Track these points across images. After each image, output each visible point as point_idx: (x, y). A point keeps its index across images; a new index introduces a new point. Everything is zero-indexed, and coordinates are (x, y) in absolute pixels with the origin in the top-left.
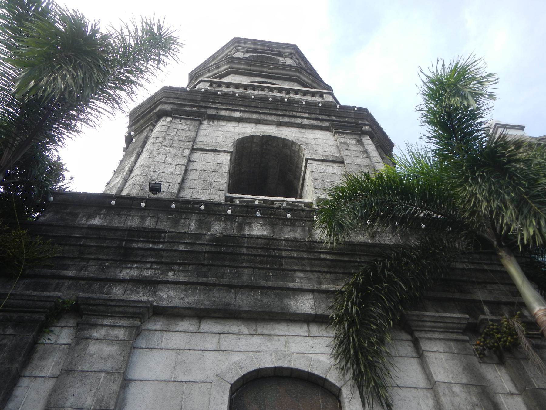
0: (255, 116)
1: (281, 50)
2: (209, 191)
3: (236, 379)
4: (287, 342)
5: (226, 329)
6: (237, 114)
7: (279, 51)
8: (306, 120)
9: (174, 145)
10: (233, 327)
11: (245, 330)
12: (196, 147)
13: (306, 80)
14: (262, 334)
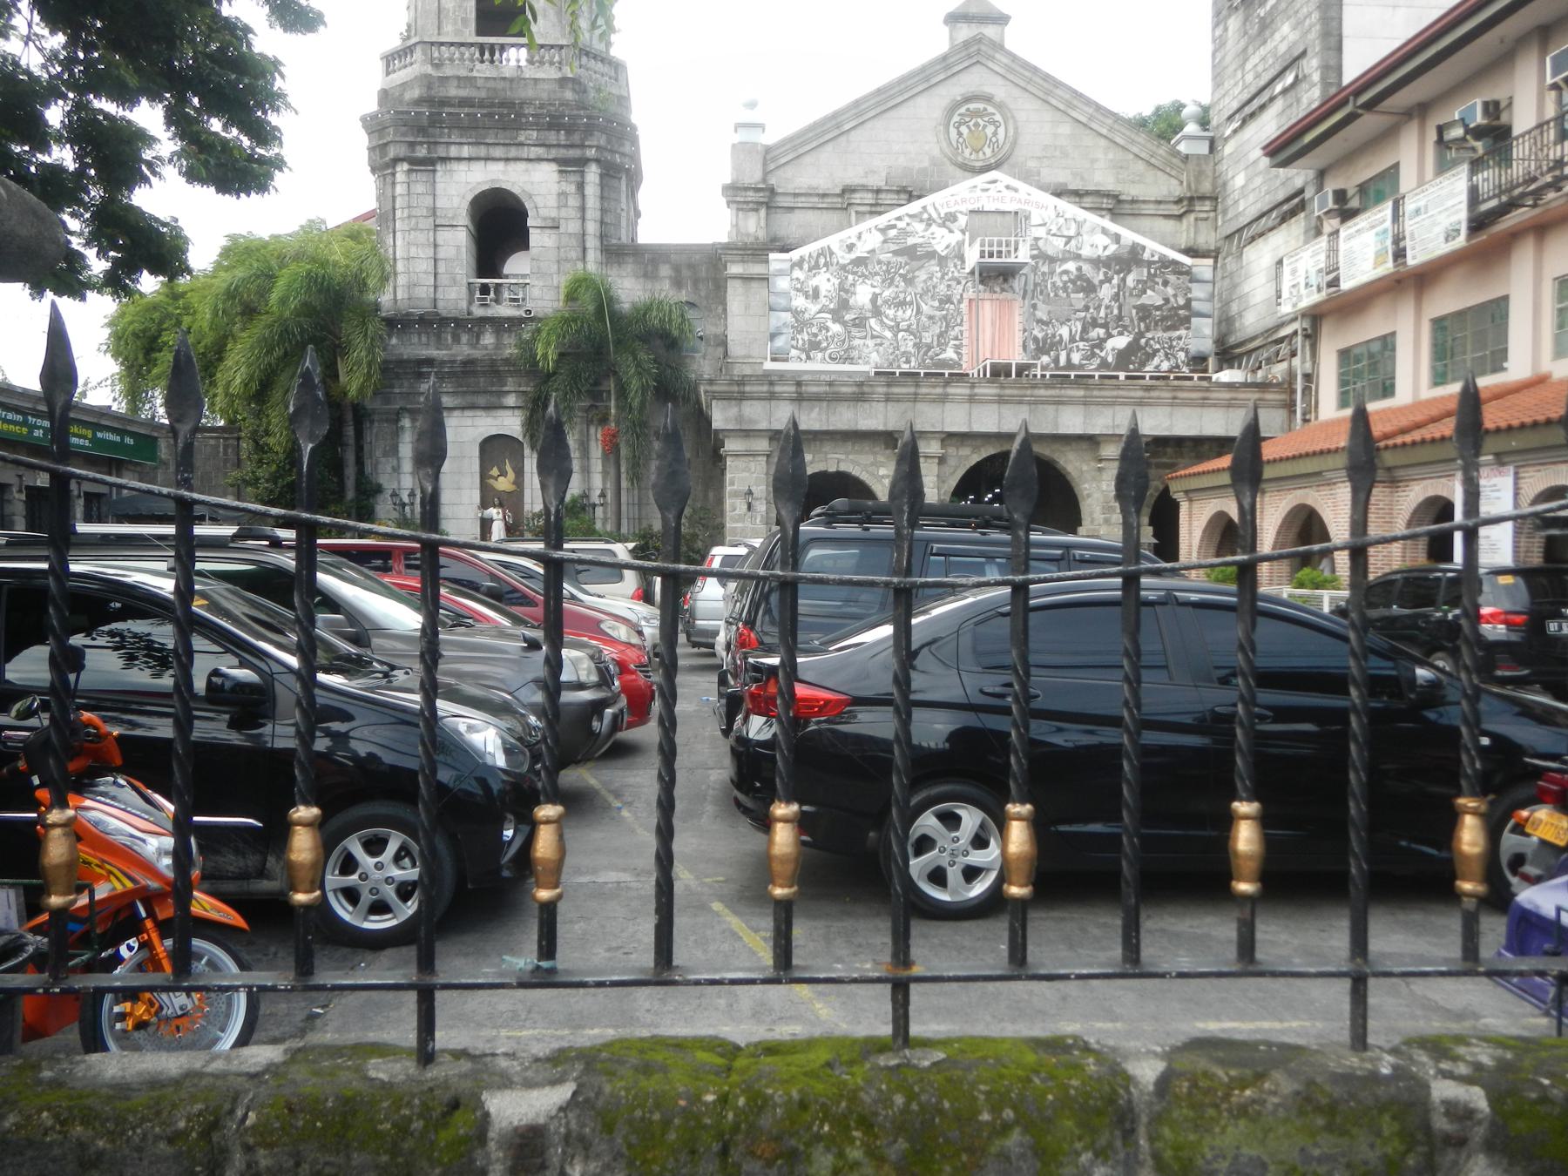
0: (482, 151)
6: (466, 151)
9: (420, 226)
10: (479, 413)
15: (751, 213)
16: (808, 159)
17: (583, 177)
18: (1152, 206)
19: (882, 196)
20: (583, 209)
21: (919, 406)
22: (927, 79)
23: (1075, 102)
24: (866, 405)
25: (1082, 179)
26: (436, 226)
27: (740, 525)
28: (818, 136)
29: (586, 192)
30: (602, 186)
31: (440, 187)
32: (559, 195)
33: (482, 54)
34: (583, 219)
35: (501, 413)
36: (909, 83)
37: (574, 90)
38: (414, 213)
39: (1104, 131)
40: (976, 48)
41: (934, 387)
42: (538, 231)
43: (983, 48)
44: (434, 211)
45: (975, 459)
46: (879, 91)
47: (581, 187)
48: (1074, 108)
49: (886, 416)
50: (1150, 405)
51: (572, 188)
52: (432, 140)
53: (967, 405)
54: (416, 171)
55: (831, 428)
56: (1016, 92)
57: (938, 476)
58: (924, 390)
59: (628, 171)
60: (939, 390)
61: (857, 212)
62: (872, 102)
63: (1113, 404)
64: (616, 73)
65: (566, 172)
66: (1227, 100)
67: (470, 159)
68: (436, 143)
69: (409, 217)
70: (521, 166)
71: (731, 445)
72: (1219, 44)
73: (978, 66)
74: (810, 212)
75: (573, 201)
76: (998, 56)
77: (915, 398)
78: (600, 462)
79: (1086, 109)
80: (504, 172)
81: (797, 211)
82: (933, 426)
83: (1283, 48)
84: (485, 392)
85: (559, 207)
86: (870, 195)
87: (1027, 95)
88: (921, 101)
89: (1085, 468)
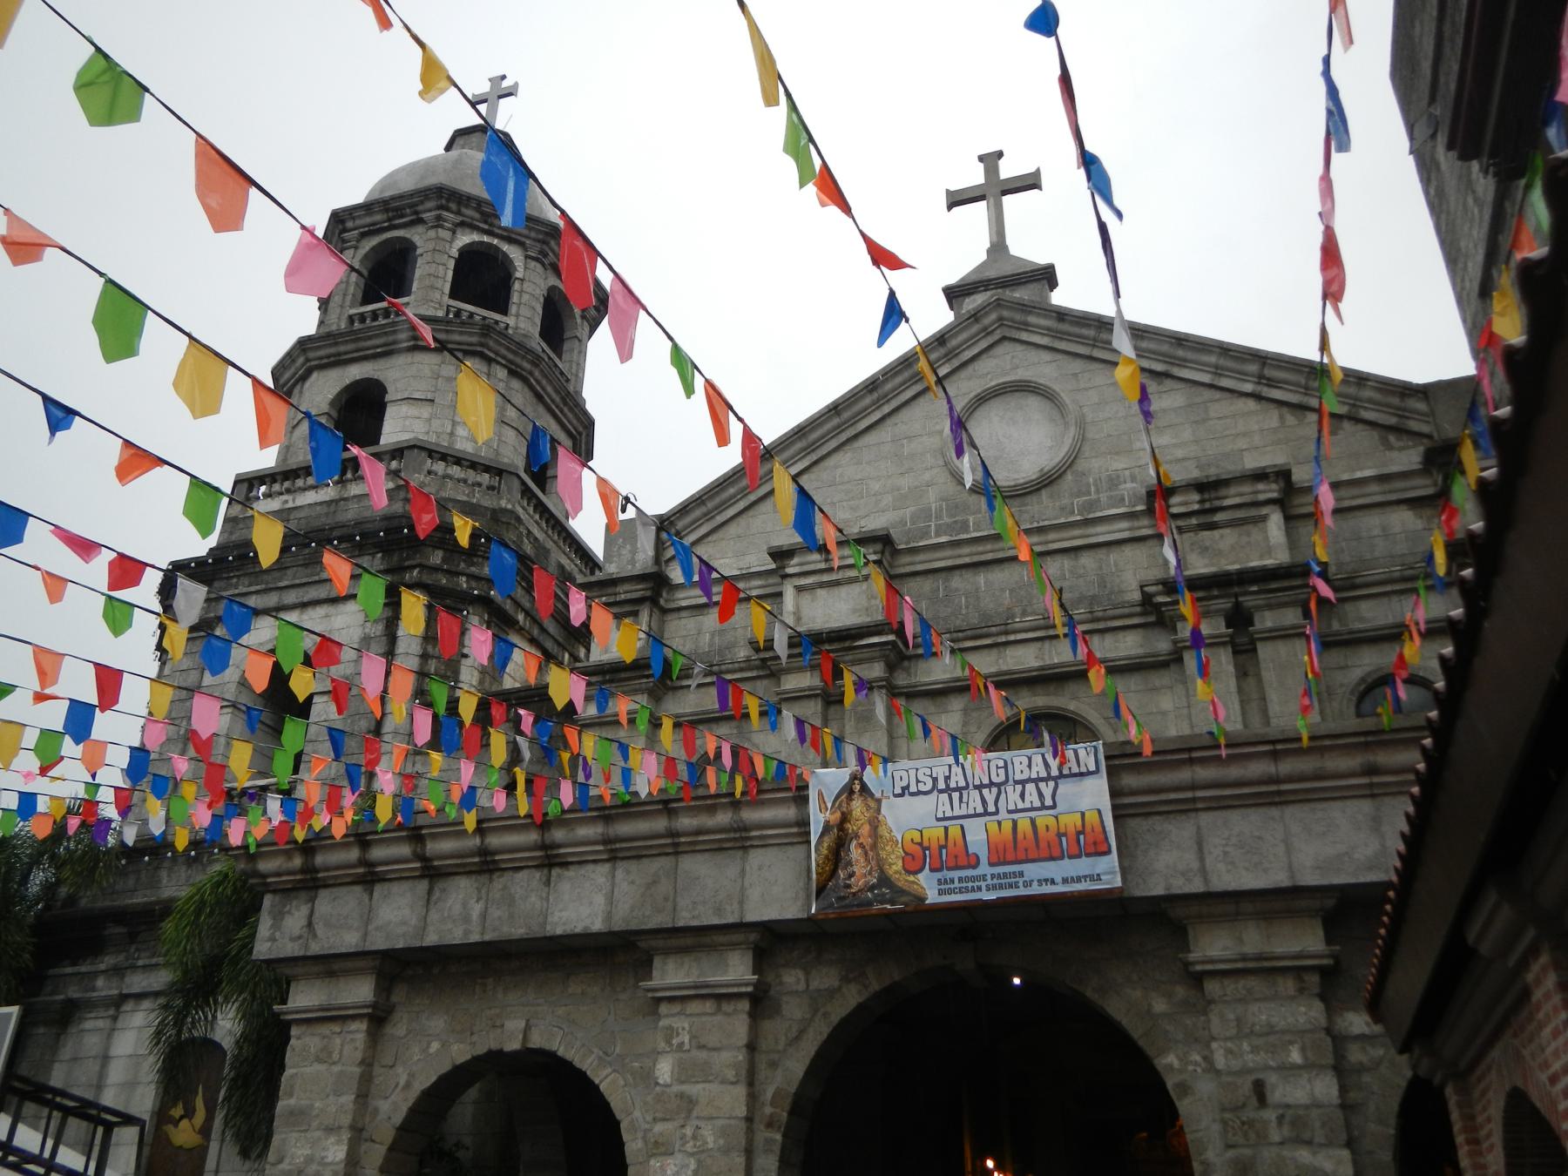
7: (416, 213)
16: (732, 529)
18: (1374, 488)
21: (689, 864)
23: (1180, 353)
24: (571, 873)
25: (1218, 467)
29: (400, 633)
36: (889, 386)
39: (1248, 387)
40: (993, 316)
41: (712, 810)
43: (1006, 313)
45: (852, 997)
46: (835, 409)
48: (1183, 363)
50: (1305, 798)
55: (487, 938)
56: (1077, 365)
57: (751, 1047)
58: (686, 822)
59: (485, 602)
60: (723, 818)
61: (800, 589)
63: (1187, 808)
66: (1470, 265)
70: (321, 611)
71: (304, 997)
72: (1437, 204)
76: (1032, 319)
77: (675, 844)
82: (719, 911)
89: (1160, 1006)
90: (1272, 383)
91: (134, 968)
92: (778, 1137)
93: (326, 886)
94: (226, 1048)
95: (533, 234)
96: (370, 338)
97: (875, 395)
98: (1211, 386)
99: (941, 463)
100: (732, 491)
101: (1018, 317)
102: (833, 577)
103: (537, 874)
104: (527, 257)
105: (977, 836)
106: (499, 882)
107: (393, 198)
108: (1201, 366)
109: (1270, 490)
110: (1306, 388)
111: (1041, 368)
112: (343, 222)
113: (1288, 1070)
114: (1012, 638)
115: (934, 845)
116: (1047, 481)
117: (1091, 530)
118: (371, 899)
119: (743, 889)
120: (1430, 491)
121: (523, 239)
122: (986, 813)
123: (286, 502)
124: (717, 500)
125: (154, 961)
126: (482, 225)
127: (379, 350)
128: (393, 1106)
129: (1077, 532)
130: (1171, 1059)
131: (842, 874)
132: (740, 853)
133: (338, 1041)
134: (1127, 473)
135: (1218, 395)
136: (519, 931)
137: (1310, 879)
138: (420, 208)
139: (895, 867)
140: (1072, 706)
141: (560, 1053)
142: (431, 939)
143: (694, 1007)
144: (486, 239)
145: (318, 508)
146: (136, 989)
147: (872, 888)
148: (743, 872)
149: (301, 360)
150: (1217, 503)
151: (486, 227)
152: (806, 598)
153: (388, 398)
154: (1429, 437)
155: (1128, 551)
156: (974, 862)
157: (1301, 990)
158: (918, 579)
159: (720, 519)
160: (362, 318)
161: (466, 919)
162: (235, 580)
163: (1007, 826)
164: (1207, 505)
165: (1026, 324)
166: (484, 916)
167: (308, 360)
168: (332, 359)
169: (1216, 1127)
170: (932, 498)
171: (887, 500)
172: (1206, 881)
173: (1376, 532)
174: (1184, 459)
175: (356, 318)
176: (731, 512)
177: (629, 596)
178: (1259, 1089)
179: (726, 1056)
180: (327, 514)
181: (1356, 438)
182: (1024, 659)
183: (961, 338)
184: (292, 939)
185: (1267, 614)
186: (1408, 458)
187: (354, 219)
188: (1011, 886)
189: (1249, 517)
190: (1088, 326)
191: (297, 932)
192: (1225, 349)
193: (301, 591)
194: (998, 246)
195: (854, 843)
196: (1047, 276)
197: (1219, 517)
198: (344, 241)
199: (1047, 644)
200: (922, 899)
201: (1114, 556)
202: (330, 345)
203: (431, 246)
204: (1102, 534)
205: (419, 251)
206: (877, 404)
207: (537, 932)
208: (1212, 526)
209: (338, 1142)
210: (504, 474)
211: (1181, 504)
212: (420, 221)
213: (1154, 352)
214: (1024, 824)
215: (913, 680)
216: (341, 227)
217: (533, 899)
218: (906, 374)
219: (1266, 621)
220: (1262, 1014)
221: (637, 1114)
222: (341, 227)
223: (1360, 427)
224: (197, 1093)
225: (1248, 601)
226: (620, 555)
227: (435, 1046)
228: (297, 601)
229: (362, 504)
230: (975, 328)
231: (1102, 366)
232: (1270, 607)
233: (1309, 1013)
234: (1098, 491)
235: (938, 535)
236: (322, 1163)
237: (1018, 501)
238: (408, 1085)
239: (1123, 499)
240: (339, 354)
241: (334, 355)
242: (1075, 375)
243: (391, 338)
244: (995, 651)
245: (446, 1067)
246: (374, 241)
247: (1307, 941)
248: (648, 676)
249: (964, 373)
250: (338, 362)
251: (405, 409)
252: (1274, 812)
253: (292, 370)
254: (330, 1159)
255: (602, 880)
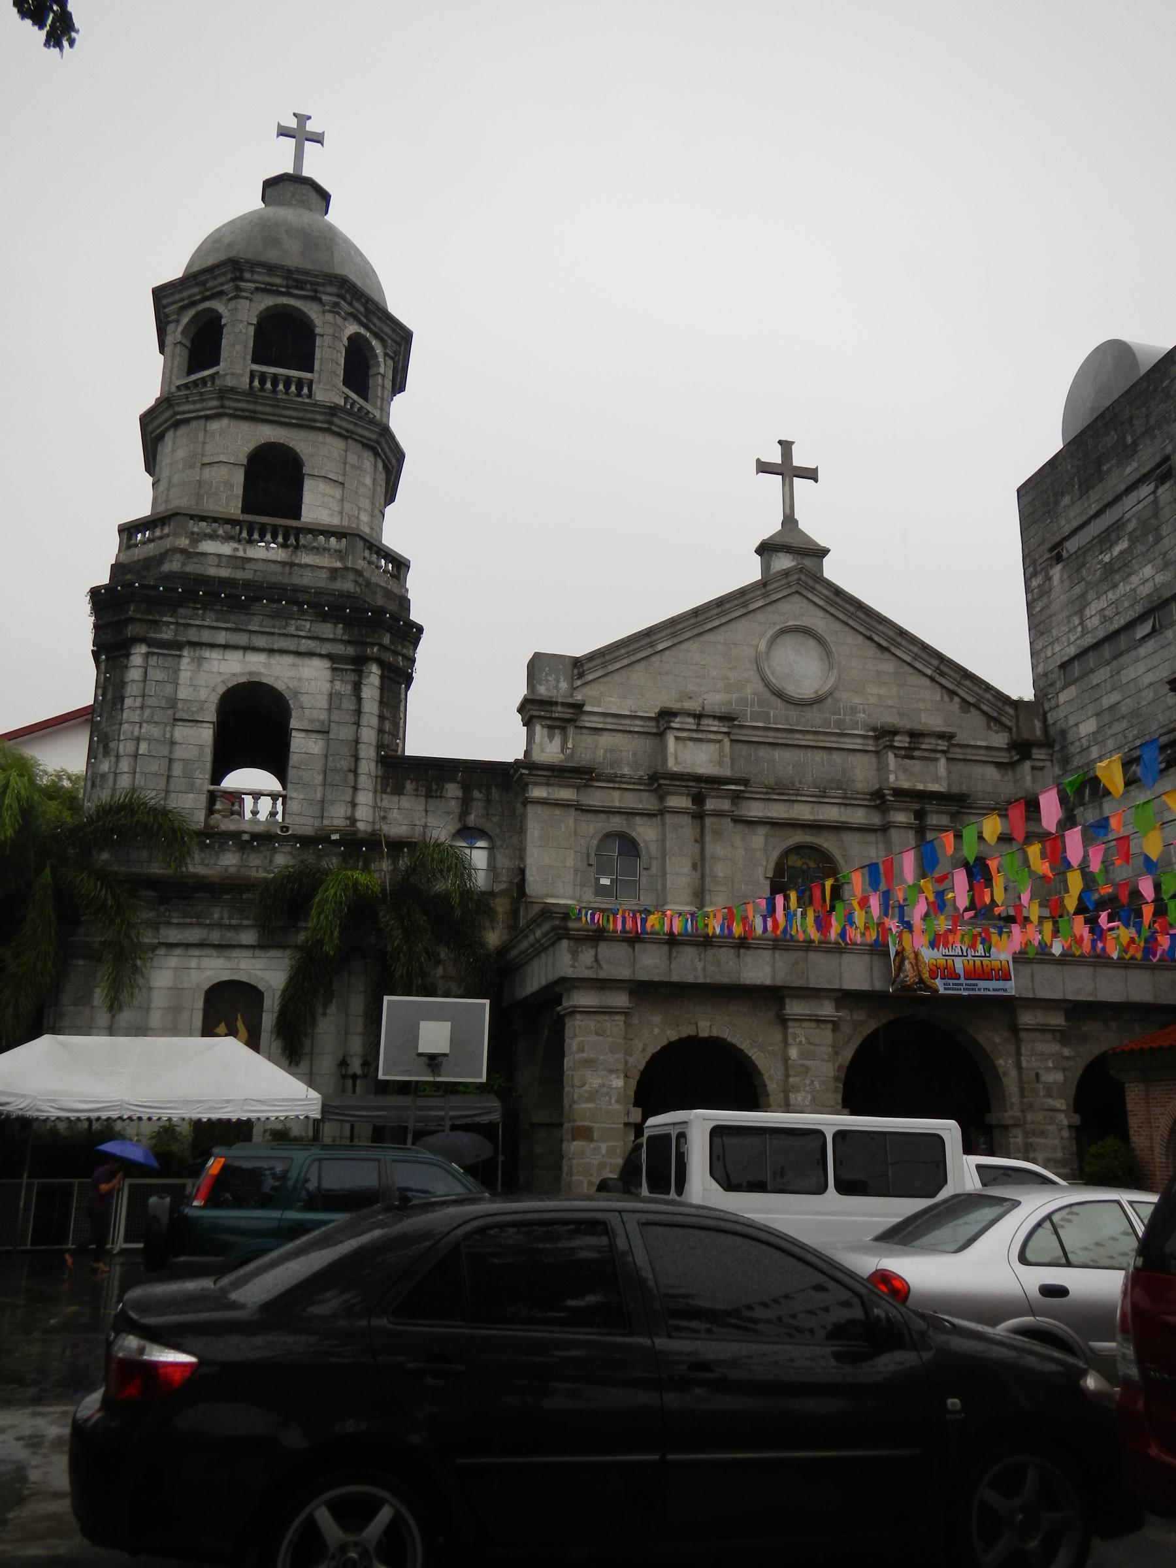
0: (242, 639)
1: (321, 289)
2: (191, 796)
3: (208, 987)
4: (239, 962)
5: (203, 953)
6: (221, 637)
7: (316, 291)
8: (304, 641)
9: (156, 719)
11: (215, 954)
12: (177, 717)
13: (345, 425)
14: (225, 957)
15: (557, 731)
16: (617, 678)
17: (360, 677)
18: (983, 752)
19: (704, 721)
20: (358, 712)
21: (812, 956)
22: (745, 604)
24: (751, 952)
26: (176, 720)
27: (590, 1105)
28: (629, 654)
29: (364, 695)
30: (382, 689)
31: (185, 675)
32: (331, 695)
33: (250, 534)
34: (358, 724)
35: (236, 953)
36: (728, 606)
37: (355, 581)
38: (149, 702)
39: (929, 672)
42: (303, 735)
43: (803, 577)
44: (173, 702)
45: (872, 1026)
46: (696, 612)
47: (357, 688)
49: (773, 968)
51: (348, 689)
52: (181, 621)
53: (867, 958)
54: (159, 654)
55: (708, 981)
56: (837, 626)
61: (677, 738)
62: (689, 622)
64: (399, 570)
65: (342, 670)
66: (1057, 648)
67: (226, 647)
68: (187, 625)
69: (142, 707)
70: (287, 660)
73: (797, 595)
74: (620, 735)
75: (349, 704)
76: (818, 587)
78: (360, 1021)
79: (912, 648)
80: (268, 665)
81: (606, 733)
83: (1145, 590)
84: (220, 925)
85: (329, 710)
86: (691, 720)
87: (847, 629)
88: (741, 627)
90: (942, 674)
91: (168, 924)
92: (841, 1086)
93: (605, 939)
94: (262, 990)
95: (394, 336)
96: (289, 408)
97: (720, 610)
98: (909, 664)
99: (755, 668)
100: (623, 651)
101: (811, 582)
102: (700, 736)
103: (732, 951)
104: (386, 354)
105: (959, 965)
106: (710, 952)
107: (298, 271)
108: (907, 651)
109: (943, 745)
110: (959, 683)
111: (817, 621)
112: (241, 271)
113: (1048, 1069)
114: (799, 798)
115: (942, 967)
116: (818, 701)
117: (842, 740)
118: (634, 951)
119: (841, 972)
120: (1006, 761)
121: (386, 338)
122: (963, 956)
123: (236, 550)
124: (613, 656)
125: (188, 920)
126: (363, 318)
127: (294, 421)
128: (640, 1061)
129: (834, 739)
130: (1001, 1062)
131: (902, 975)
132: (837, 954)
133: (608, 1025)
134: (861, 707)
135: (912, 671)
136: (725, 980)
137: (1070, 997)
138: (321, 289)
139: (926, 975)
140: (826, 845)
141: (729, 1039)
142: (675, 978)
143: (805, 1024)
144: (362, 331)
145: (273, 566)
146: (171, 940)
147: (916, 984)
148: (840, 964)
149: (215, 403)
150: (917, 745)
151: (365, 321)
152: (680, 744)
153: (305, 470)
154: (1010, 729)
155: (859, 757)
156: (957, 977)
157: (1054, 1038)
158: (739, 744)
159: (611, 668)
160: (263, 378)
161: (695, 970)
162: (201, 612)
163: (971, 963)
164: (912, 746)
165: (814, 588)
166: (704, 969)
167: (223, 406)
168: (247, 414)
169: (1016, 1089)
170: (749, 690)
171: (720, 685)
172: (1034, 994)
173: (980, 777)
174: (891, 707)
175: (257, 374)
176: (618, 665)
177: (561, 715)
178: (1037, 1076)
179: (823, 1049)
180: (283, 574)
181: (976, 718)
182: (804, 812)
183: (775, 585)
184: (586, 968)
185: (934, 816)
186: (1000, 740)
187: (253, 272)
188: (973, 990)
189: (930, 758)
190: (851, 604)
191: (589, 964)
192: (925, 647)
193: (270, 639)
194: (789, 520)
195: (906, 962)
196: (824, 552)
197: (916, 753)
198: (238, 288)
199: (816, 806)
200: (937, 991)
201: (851, 758)
202: (249, 402)
203: (329, 330)
204: (848, 743)
205: (318, 331)
206: (719, 615)
207: (735, 981)
208: (911, 758)
209: (618, 1078)
210: (403, 567)
211: (899, 741)
212: (319, 300)
213: (884, 634)
214: (978, 963)
215: (741, 813)
216: (238, 274)
217: (731, 963)
218: (740, 601)
219: (933, 820)
220: (1041, 1047)
221: (772, 1071)
222: (238, 274)
223: (978, 712)
224: (237, 1019)
225: (928, 807)
226: (547, 681)
227: (656, 1031)
228: (267, 646)
229: (315, 574)
230: (785, 581)
231: (851, 631)
232: (937, 813)
233: (1054, 1048)
234: (844, 714)
235: (752, 720)
236: (610, 1087)
237: (799, 708)
238: (644, 1050)
239: (857, 723)
240: (255, 412)
241: (250, 411)
242: (836, 632)
243: (309, 416)
244: (787, 804)
245: (664, 1042)
246: (269, 301)
247: (1057, 1020)
248: (582, 779)
249: (770, 608)
250: (253, 418)
251: (322, 486)
252: (1060, 967)
253: (198, 406)
254: (615, 1086)
255: (768, 959)
